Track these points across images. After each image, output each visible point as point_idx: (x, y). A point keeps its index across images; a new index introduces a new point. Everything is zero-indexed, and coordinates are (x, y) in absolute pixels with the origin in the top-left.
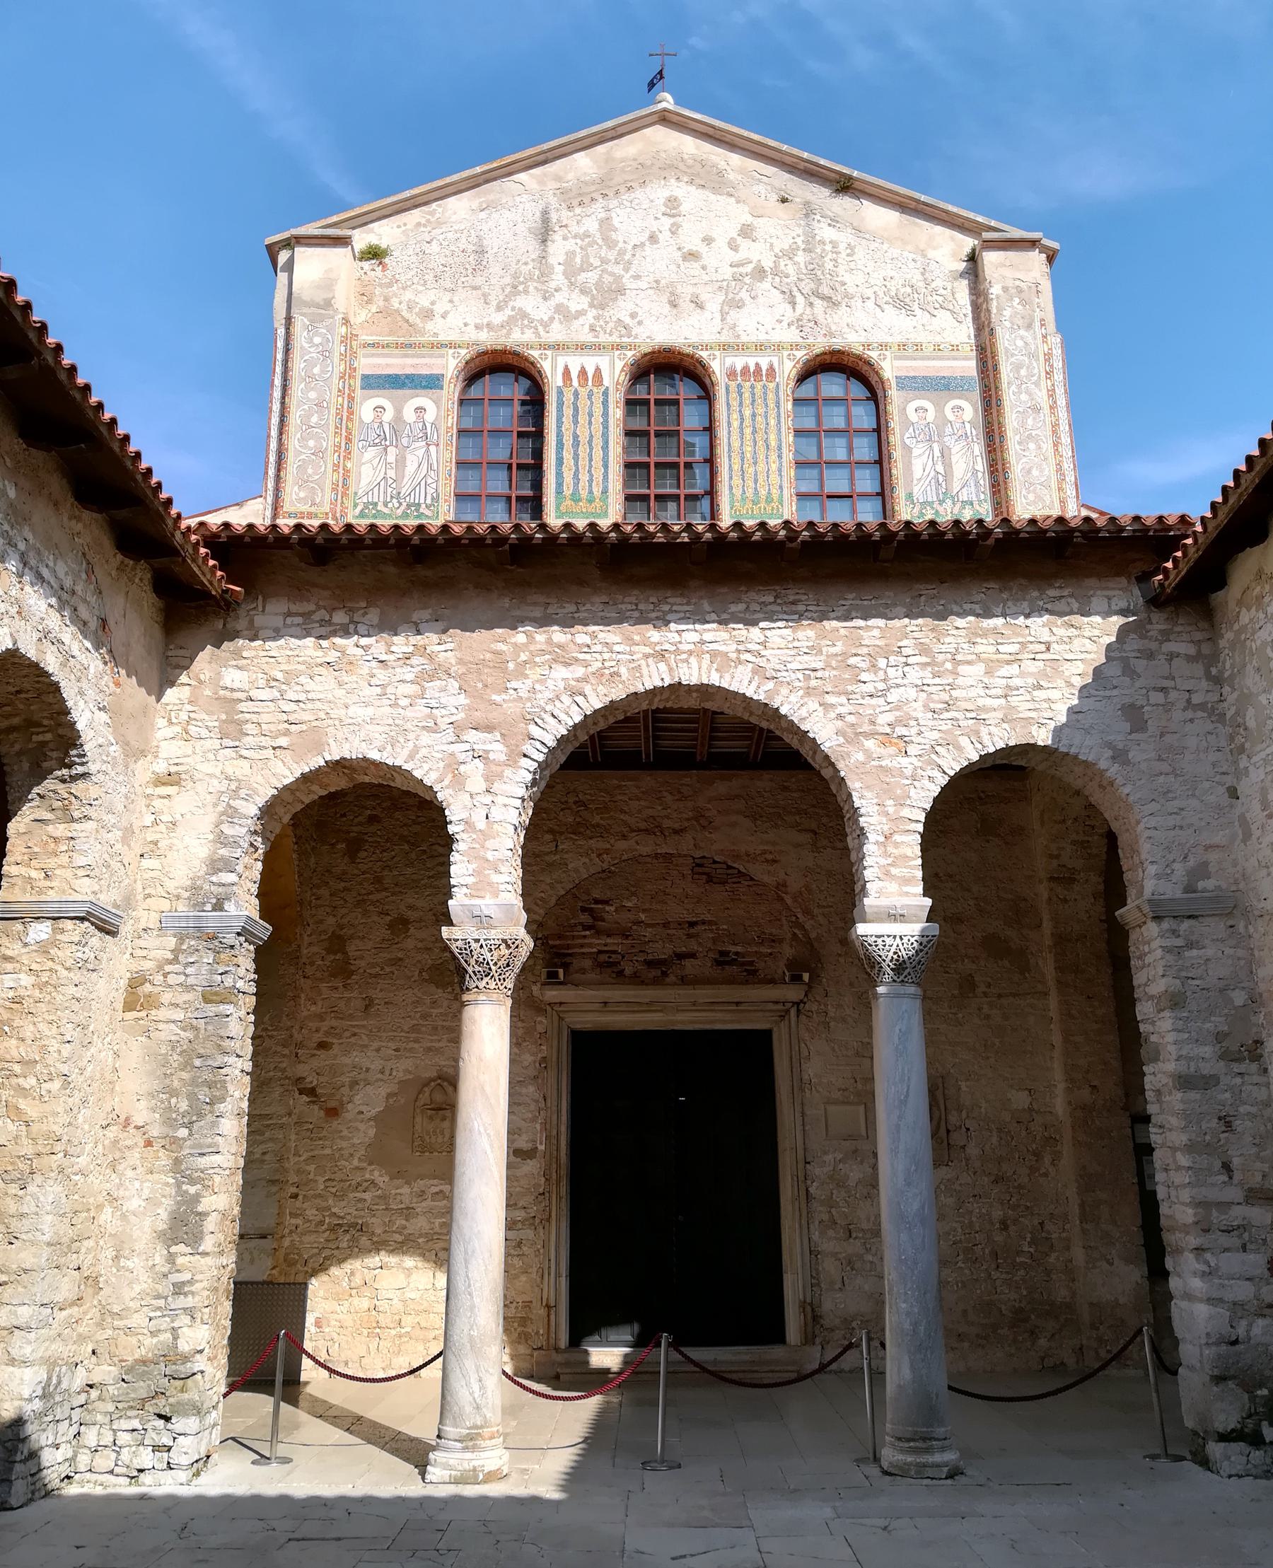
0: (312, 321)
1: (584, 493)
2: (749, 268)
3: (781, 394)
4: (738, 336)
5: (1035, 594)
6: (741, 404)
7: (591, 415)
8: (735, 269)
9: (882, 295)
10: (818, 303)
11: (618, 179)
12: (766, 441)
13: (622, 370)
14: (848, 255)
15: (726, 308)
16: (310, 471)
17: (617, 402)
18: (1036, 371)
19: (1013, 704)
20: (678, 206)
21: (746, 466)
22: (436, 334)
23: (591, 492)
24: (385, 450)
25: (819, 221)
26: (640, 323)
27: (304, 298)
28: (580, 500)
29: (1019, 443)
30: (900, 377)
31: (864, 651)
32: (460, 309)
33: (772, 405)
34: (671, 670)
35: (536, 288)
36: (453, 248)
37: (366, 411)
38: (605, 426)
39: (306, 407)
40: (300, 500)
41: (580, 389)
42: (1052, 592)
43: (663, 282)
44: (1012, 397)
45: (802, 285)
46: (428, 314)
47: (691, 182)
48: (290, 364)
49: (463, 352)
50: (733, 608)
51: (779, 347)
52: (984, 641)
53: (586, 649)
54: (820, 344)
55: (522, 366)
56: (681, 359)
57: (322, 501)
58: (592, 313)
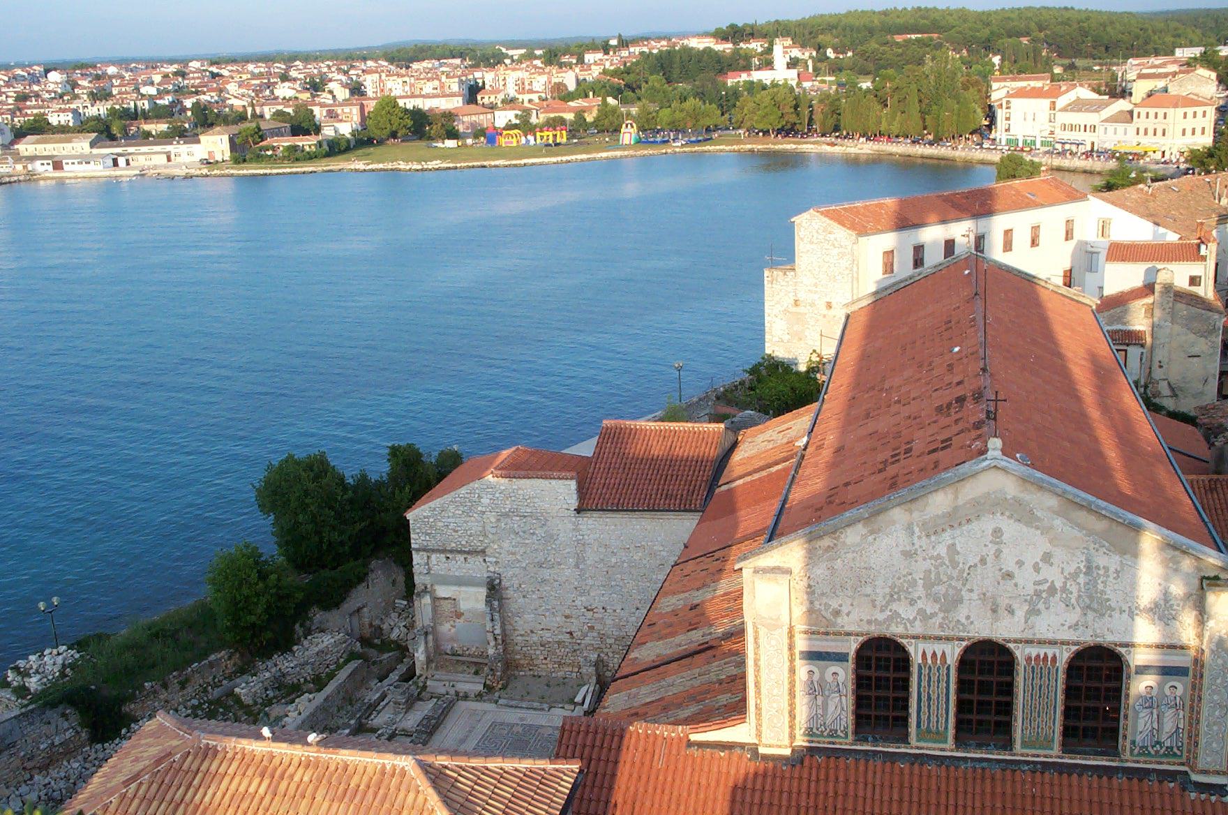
2: (1045, 586)
7: (939, 682)
8: (1036, 587)
10: (1091, 615)
20: (1002, 535)
22: (843, 626)
26: (972, 623)
46: (837, 613)
47: (1010, 517)
51: (1063, 643)
58: (941, 615)
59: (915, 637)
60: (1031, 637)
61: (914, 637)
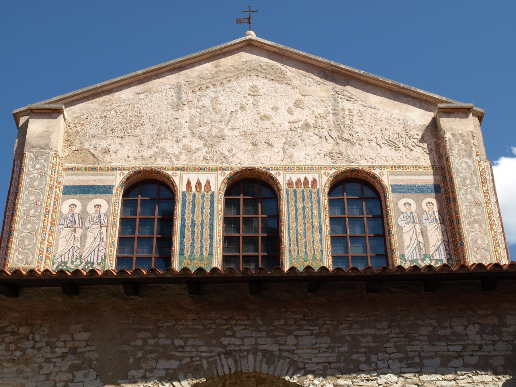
0: (36, 156)
1: (197, 255)
2: (300, 124)
3: (321, 195)
4: (294, 162)
5: (470, 313)
6: (296, 201)
7: (203, 208)
8: (292, 125)
9: (379, 139)
10: (343, 144)
11: (222, 76)
12: (312, 223)
13: (223, 182)
14: (359, 117)
15: (286, 146)
16: (26, 243)
17: (219, 201)
18: (475, 181)
19: (460, 385)
21: (299, 238)
23: (202, 254)
24: (75, 230)
25: (341, 98)
27: (32, 143)
28: (194, 259)
29: (469, 224)
30: (394, 185)
31: (363, 350)
32: (126, 148)
33: (315, 202)
34: (236, 362)
35: (172, 136)
36: (123, 114)
37: (65, 208)
38: (212, 215)
39: (28, 205)
40: (18, 260)
41: (196, 193)
42: (480, 312)
43: (248, 132)
44: (462, 197)
45: (332, 133)
46: (107, 151)
48: (20, 180)
49: (126, 172)
50: (276, 323)
51: (319, 168)
52: (439, 343)
53: (180, 350)
54: (344, 165)
55: (162, 180)
56: (259, 176)
57: (33, 261)
59: (182, 169)
60: (291, 165)
61: (178, 169)
